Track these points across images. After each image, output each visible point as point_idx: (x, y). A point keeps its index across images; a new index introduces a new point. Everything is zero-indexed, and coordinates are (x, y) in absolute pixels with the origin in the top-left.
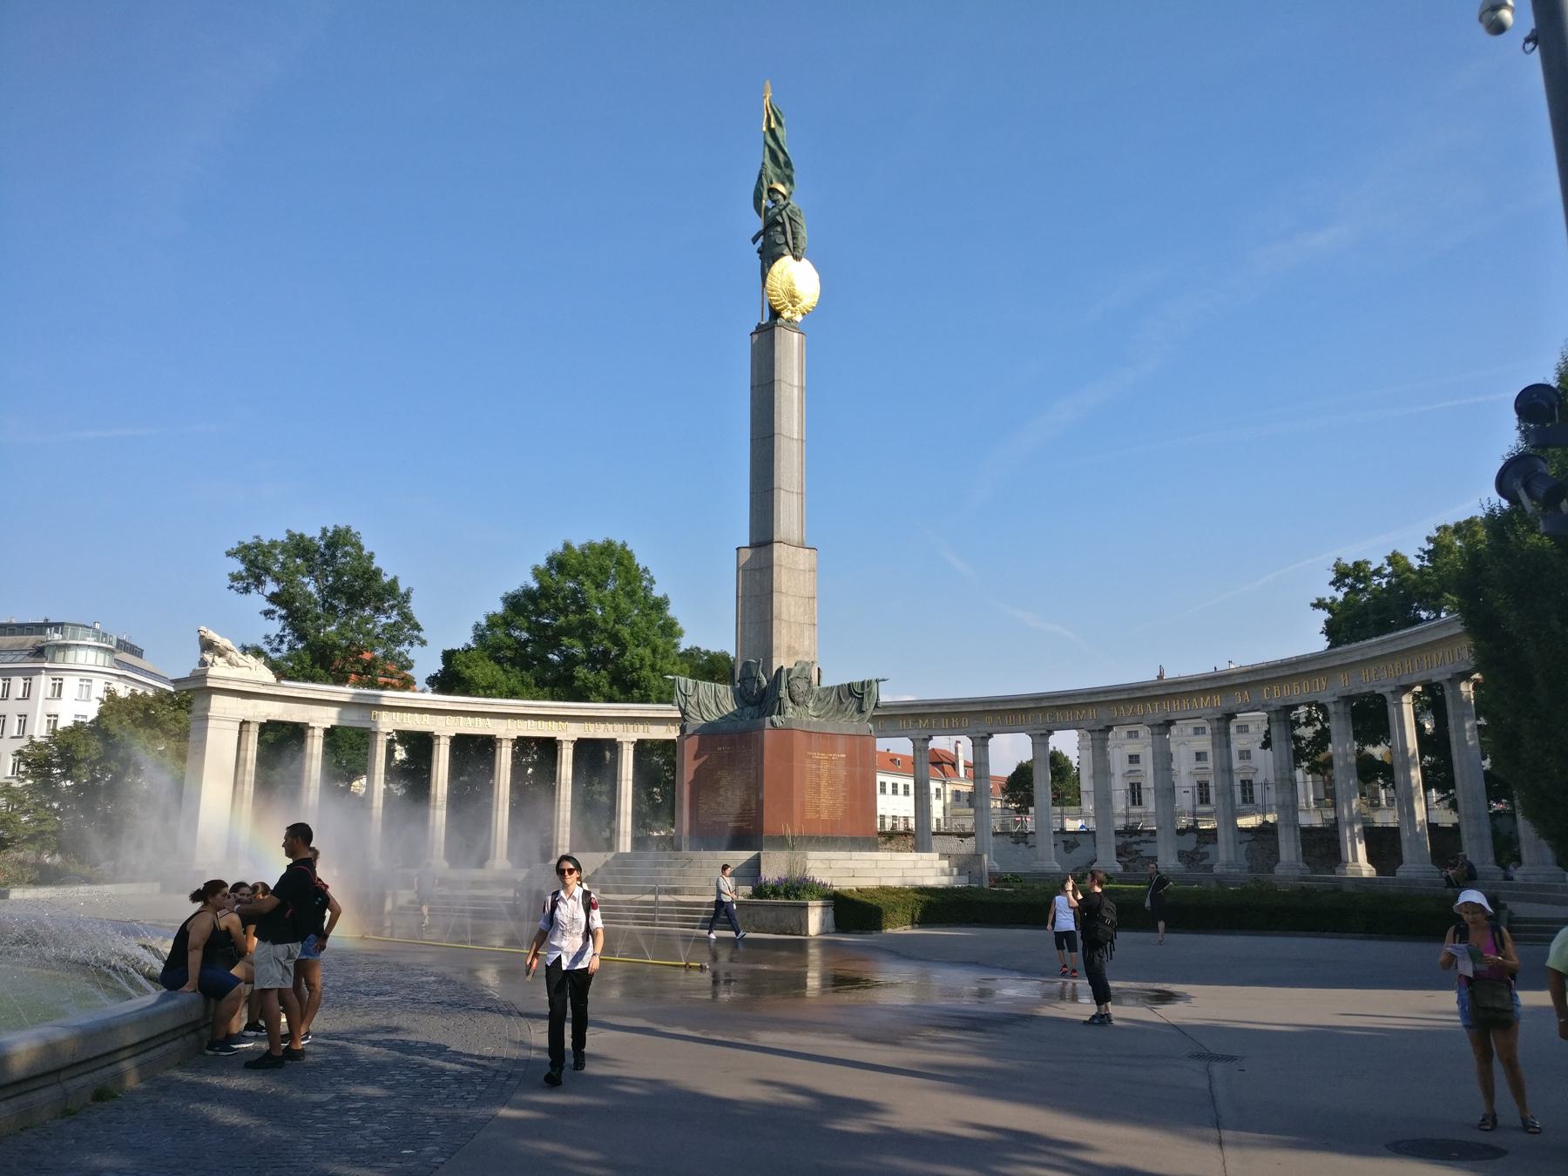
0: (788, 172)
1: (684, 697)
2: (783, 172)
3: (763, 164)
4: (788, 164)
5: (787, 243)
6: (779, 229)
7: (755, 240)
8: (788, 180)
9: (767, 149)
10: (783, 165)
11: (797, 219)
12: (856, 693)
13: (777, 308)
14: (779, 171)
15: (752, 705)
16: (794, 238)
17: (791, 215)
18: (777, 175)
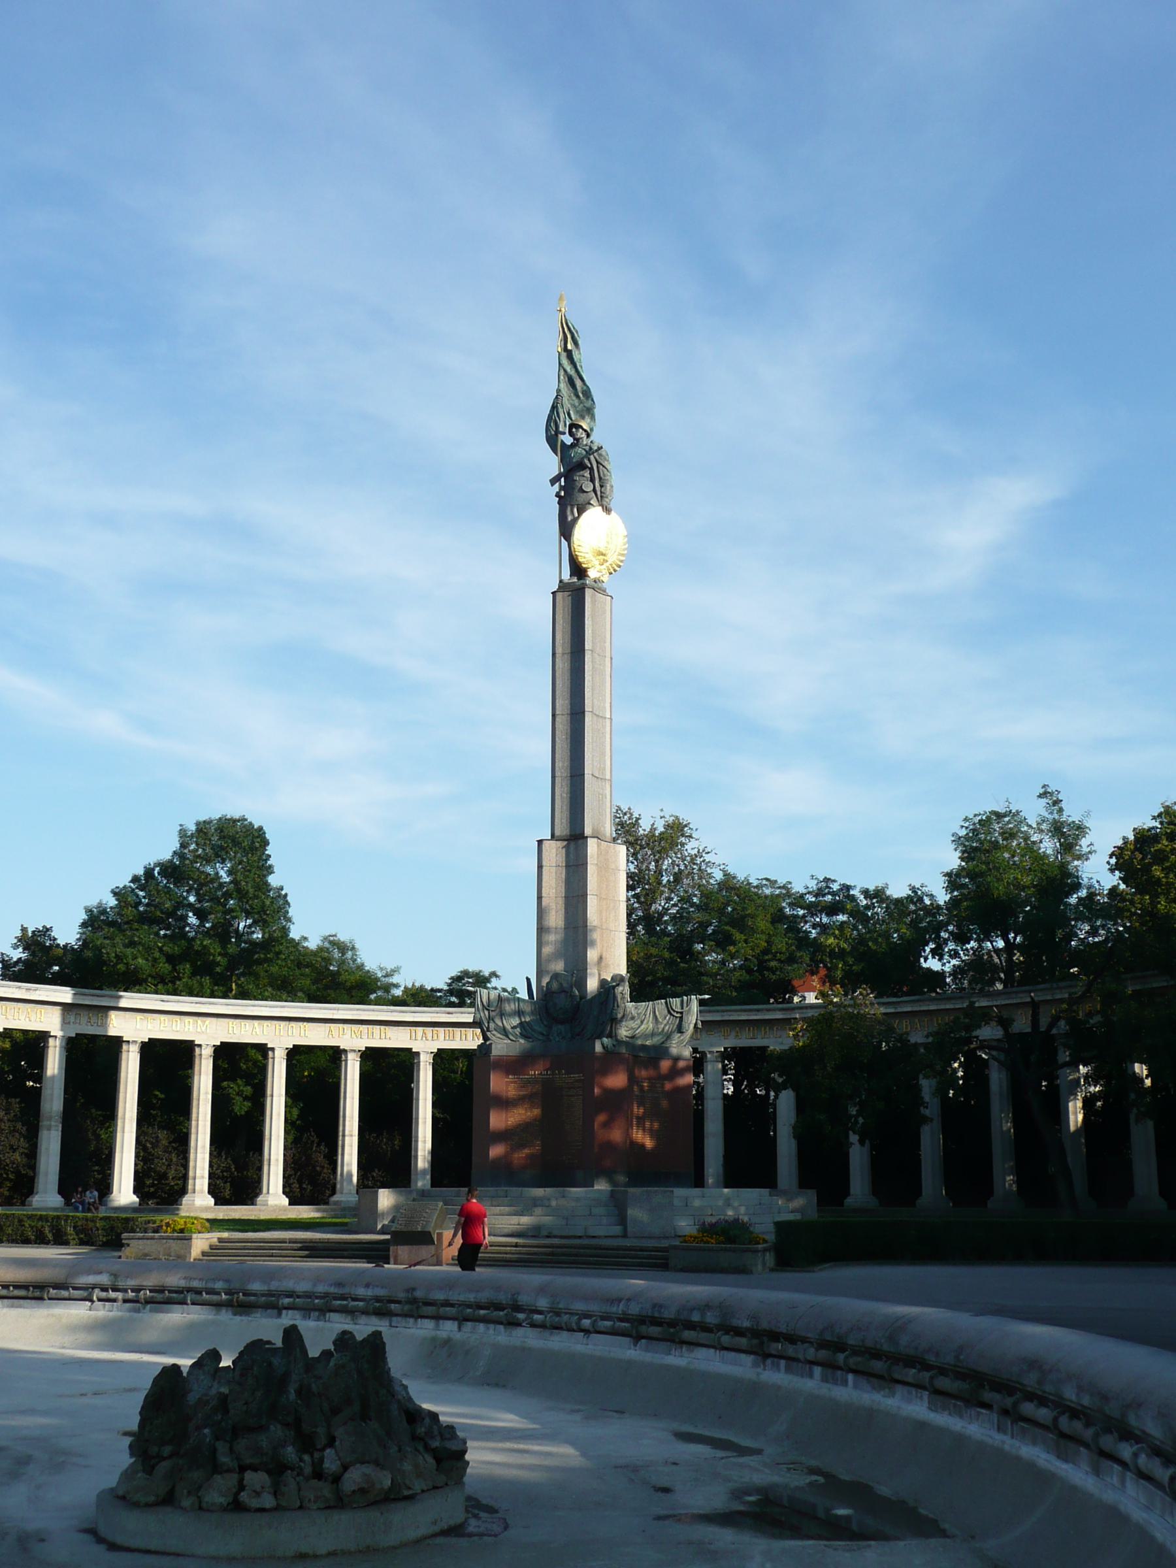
0: (588, 404)
1: (486, 1013)
2: (581, 402)
3: (559, 391)
4: (587, 393)
5: (594, 490)
6: (587, 474)
7: (553, 481)
8: (589, 412)
9: (562, 373)
10: (581, 395)
11: (605, 464)
12: (674, 1011)
13: (584, 566)
14: (576, 402)
15: (562, 1022)
16: (601, 486)
17: (599, 460)
18: (573, 406)
